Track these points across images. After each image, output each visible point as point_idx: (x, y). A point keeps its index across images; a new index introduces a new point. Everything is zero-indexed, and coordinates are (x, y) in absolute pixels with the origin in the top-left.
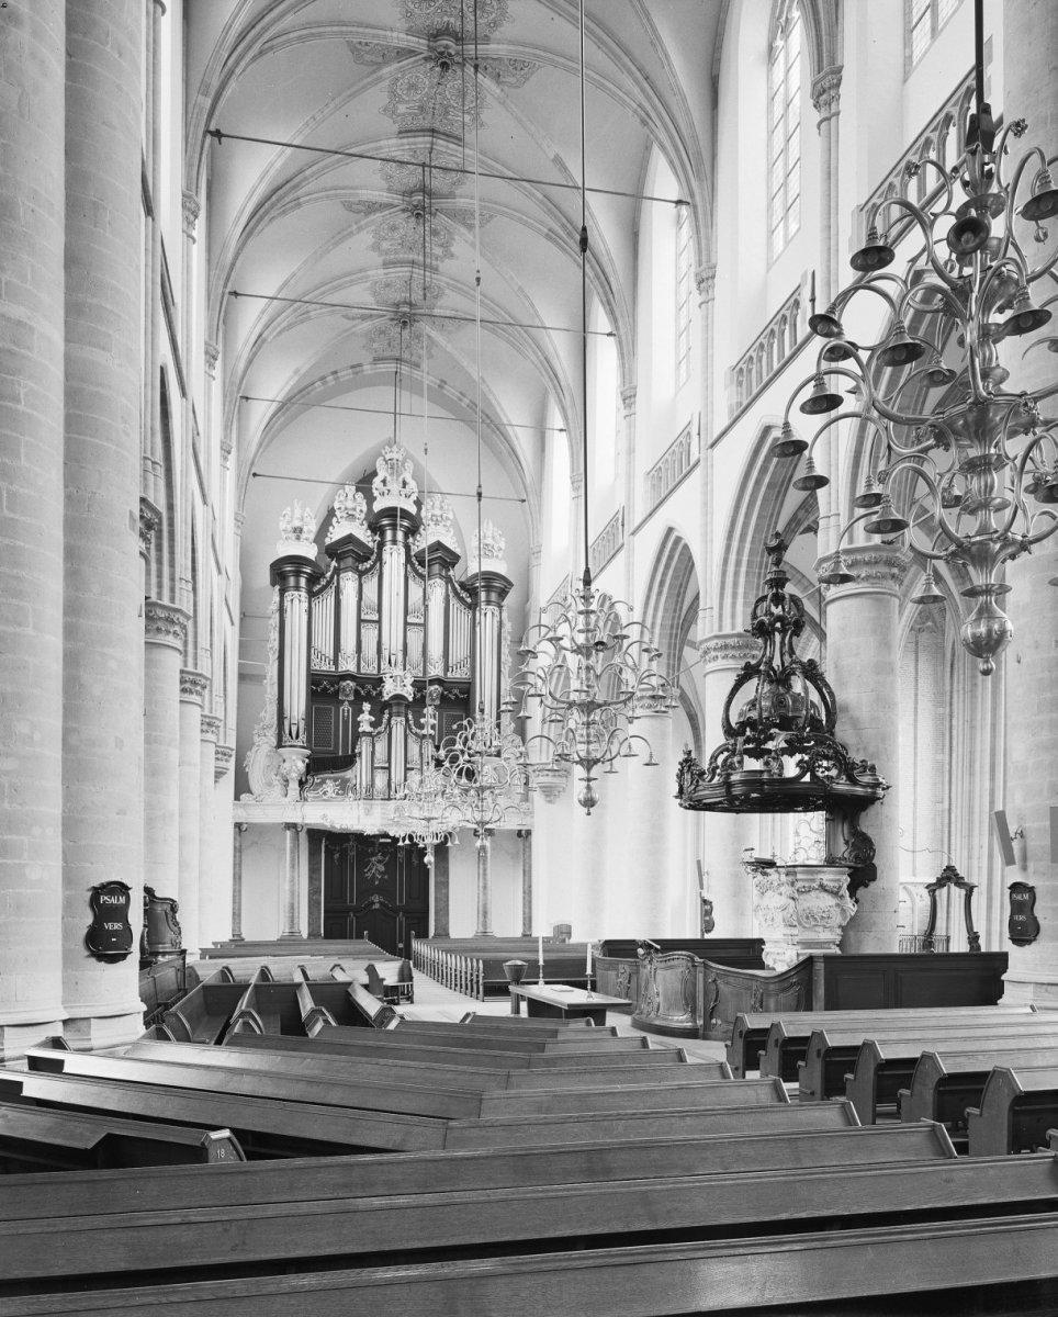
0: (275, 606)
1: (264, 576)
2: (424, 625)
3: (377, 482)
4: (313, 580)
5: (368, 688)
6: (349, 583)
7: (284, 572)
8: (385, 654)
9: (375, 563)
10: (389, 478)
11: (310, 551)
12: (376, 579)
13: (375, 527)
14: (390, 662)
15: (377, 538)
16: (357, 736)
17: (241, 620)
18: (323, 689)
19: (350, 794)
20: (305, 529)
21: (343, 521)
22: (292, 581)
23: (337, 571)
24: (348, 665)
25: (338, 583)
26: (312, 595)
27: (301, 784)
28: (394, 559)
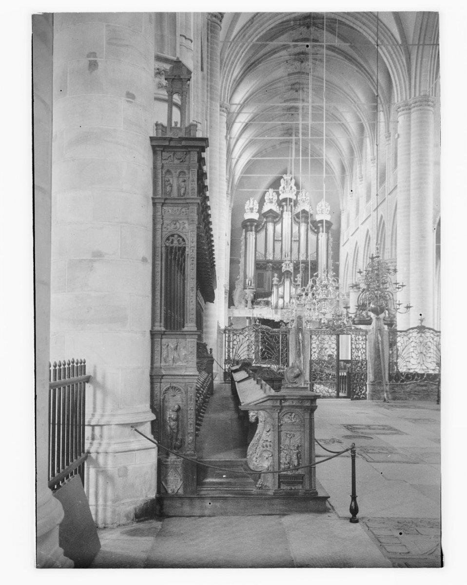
0: (243, 237)
1: (239, 225)
2: (299, 241)
3: (281, 188)
4: (257, 227)
5: (277, 266)
6: (270, 226)
8: (284, 252)
9: (280, 219)
10: (286, 186)
11: (255, 216)
12: (280, 224)
14: (285, 256)
15: (281, 209)
16: (272, 286)
17: (231, 244)
18: (260, 266)
19: (270, 306)
20: (254, 208)
21: (268, 204)
22: (249, 227)
23: (266, 222)
24: (271, 258)
25: (266, 227)
26: (257, 232)
27: (252, 302)
28: (287, 217)
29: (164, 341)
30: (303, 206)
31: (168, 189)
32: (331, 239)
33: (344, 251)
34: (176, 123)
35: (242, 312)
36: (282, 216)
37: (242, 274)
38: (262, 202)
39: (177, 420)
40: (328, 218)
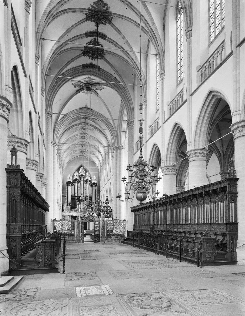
1: (65, 183)
3: (80, 171)
4: (72, 184)
5: (78, 198)
6: (76, 184)
7: (68, 183)
11: (71, 181)
13: (80, 177)
18: (73, 198)
26: (71, 186)
27: (70, 210)
28: (82, 181)
29: (11, 227)
30: (88, 177)
31: (11, 183)
32: (97, 189)
33: (101, 193)
34: (14, 164)
35: (66, 213)
36: (80, 181)
37: (66, 200)
38: (73, 176)
39: (15, 249)
40: (96, 182)
